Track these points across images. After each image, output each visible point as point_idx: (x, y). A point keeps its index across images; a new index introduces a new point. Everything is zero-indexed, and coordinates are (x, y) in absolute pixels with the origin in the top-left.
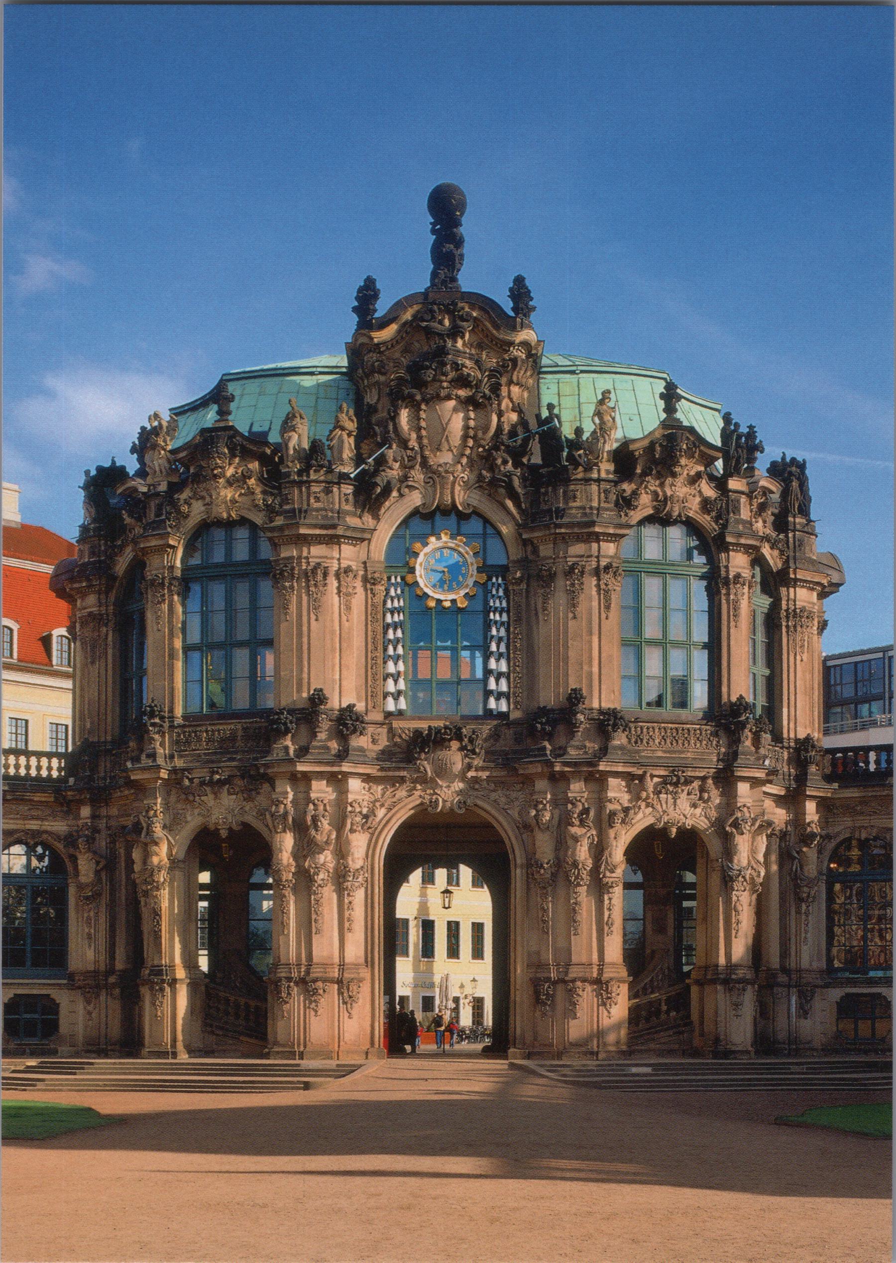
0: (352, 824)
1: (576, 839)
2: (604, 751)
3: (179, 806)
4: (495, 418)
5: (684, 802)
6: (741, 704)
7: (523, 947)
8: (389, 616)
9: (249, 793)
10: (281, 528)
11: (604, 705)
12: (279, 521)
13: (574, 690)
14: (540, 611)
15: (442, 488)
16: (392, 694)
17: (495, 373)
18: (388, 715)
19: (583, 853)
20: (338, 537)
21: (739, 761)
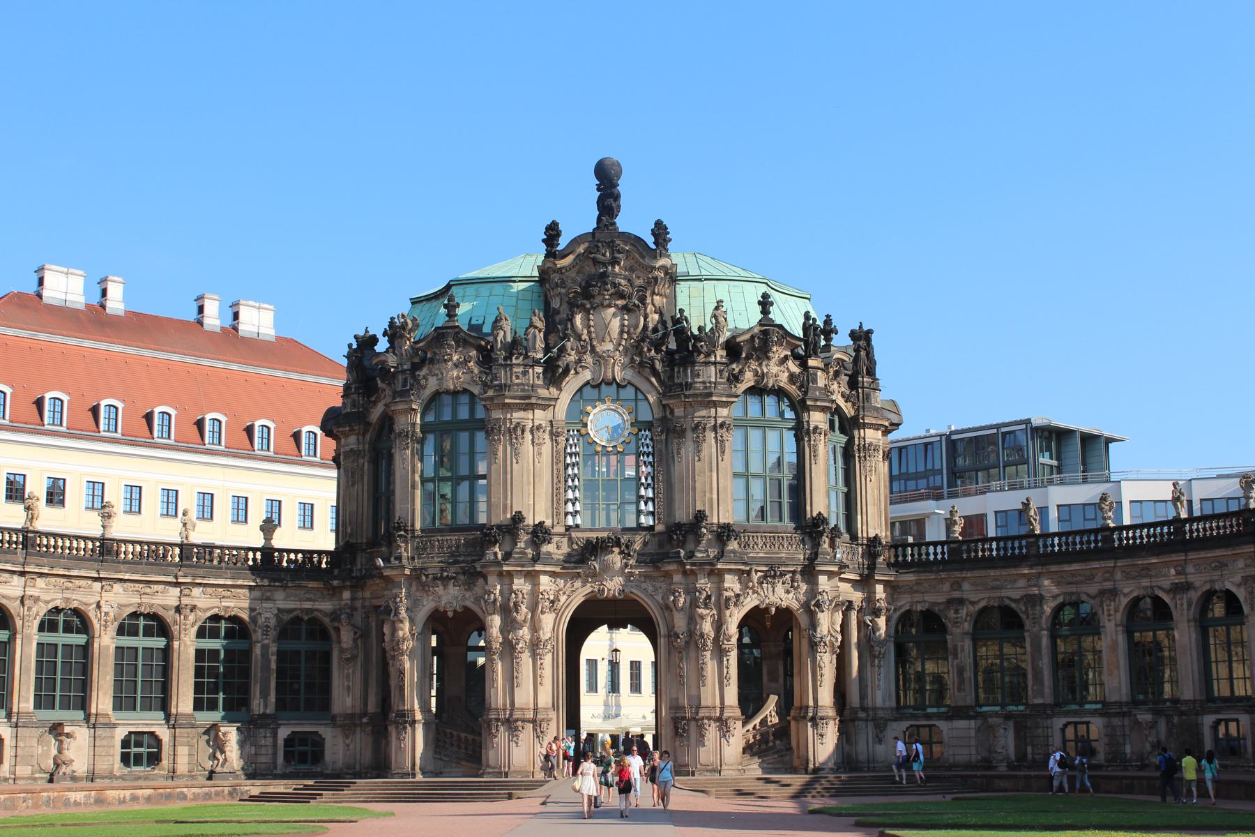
0: (542, 608)
1: (702, 617)
2: (721, 555)
3: (418, 594)
4: (642, 319)
5: (780, 589)
6: (819, 518)
7: (666, 695)
8: (568, 458)
9: (470, 585)
10: (492, 398)
11: (721, 521)
12: (490, 393)
13: (699, 511)
14: (675, 454)
15: (606, 368)
16: (571, 513)
17: (642, 289)
18: (568, 528)
19: (707, 627)
20: (532, 404)
21: (819, 559)
